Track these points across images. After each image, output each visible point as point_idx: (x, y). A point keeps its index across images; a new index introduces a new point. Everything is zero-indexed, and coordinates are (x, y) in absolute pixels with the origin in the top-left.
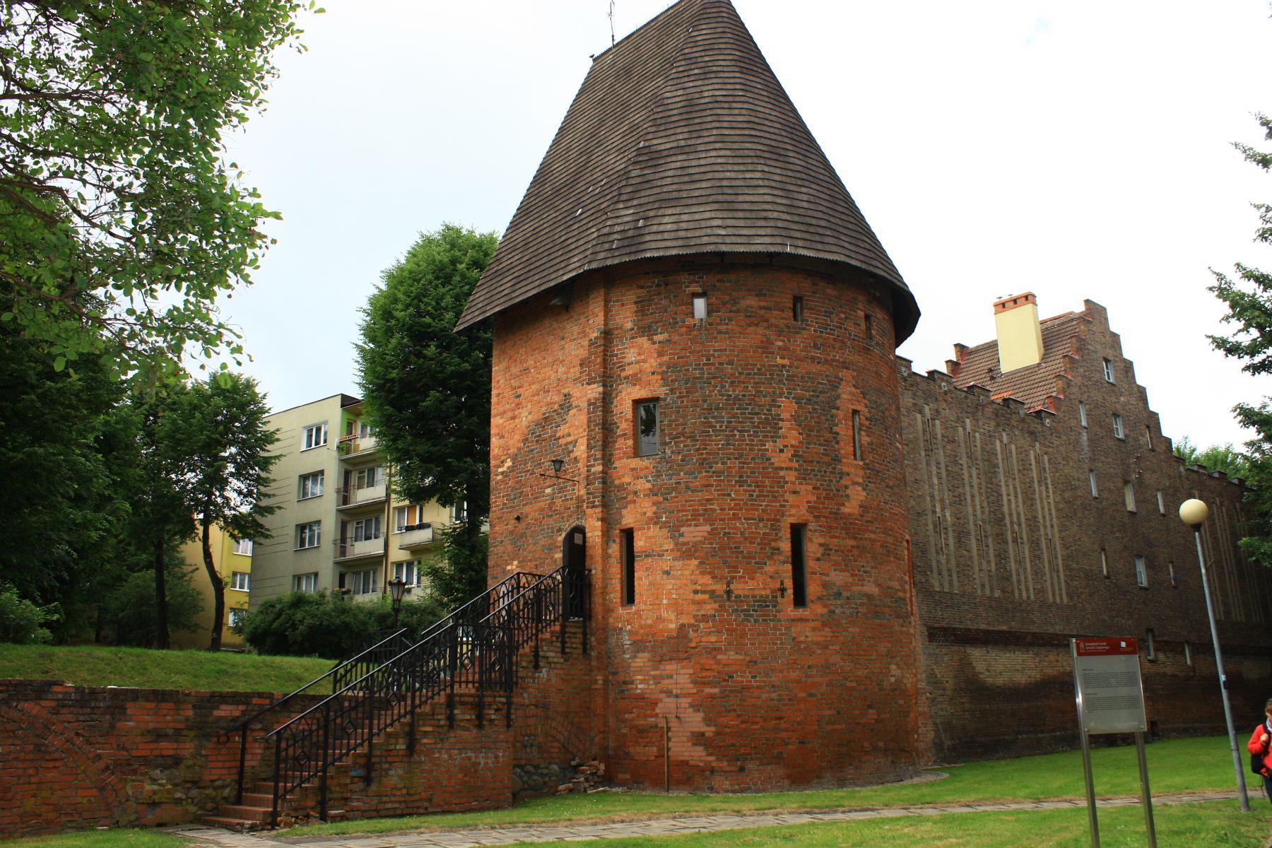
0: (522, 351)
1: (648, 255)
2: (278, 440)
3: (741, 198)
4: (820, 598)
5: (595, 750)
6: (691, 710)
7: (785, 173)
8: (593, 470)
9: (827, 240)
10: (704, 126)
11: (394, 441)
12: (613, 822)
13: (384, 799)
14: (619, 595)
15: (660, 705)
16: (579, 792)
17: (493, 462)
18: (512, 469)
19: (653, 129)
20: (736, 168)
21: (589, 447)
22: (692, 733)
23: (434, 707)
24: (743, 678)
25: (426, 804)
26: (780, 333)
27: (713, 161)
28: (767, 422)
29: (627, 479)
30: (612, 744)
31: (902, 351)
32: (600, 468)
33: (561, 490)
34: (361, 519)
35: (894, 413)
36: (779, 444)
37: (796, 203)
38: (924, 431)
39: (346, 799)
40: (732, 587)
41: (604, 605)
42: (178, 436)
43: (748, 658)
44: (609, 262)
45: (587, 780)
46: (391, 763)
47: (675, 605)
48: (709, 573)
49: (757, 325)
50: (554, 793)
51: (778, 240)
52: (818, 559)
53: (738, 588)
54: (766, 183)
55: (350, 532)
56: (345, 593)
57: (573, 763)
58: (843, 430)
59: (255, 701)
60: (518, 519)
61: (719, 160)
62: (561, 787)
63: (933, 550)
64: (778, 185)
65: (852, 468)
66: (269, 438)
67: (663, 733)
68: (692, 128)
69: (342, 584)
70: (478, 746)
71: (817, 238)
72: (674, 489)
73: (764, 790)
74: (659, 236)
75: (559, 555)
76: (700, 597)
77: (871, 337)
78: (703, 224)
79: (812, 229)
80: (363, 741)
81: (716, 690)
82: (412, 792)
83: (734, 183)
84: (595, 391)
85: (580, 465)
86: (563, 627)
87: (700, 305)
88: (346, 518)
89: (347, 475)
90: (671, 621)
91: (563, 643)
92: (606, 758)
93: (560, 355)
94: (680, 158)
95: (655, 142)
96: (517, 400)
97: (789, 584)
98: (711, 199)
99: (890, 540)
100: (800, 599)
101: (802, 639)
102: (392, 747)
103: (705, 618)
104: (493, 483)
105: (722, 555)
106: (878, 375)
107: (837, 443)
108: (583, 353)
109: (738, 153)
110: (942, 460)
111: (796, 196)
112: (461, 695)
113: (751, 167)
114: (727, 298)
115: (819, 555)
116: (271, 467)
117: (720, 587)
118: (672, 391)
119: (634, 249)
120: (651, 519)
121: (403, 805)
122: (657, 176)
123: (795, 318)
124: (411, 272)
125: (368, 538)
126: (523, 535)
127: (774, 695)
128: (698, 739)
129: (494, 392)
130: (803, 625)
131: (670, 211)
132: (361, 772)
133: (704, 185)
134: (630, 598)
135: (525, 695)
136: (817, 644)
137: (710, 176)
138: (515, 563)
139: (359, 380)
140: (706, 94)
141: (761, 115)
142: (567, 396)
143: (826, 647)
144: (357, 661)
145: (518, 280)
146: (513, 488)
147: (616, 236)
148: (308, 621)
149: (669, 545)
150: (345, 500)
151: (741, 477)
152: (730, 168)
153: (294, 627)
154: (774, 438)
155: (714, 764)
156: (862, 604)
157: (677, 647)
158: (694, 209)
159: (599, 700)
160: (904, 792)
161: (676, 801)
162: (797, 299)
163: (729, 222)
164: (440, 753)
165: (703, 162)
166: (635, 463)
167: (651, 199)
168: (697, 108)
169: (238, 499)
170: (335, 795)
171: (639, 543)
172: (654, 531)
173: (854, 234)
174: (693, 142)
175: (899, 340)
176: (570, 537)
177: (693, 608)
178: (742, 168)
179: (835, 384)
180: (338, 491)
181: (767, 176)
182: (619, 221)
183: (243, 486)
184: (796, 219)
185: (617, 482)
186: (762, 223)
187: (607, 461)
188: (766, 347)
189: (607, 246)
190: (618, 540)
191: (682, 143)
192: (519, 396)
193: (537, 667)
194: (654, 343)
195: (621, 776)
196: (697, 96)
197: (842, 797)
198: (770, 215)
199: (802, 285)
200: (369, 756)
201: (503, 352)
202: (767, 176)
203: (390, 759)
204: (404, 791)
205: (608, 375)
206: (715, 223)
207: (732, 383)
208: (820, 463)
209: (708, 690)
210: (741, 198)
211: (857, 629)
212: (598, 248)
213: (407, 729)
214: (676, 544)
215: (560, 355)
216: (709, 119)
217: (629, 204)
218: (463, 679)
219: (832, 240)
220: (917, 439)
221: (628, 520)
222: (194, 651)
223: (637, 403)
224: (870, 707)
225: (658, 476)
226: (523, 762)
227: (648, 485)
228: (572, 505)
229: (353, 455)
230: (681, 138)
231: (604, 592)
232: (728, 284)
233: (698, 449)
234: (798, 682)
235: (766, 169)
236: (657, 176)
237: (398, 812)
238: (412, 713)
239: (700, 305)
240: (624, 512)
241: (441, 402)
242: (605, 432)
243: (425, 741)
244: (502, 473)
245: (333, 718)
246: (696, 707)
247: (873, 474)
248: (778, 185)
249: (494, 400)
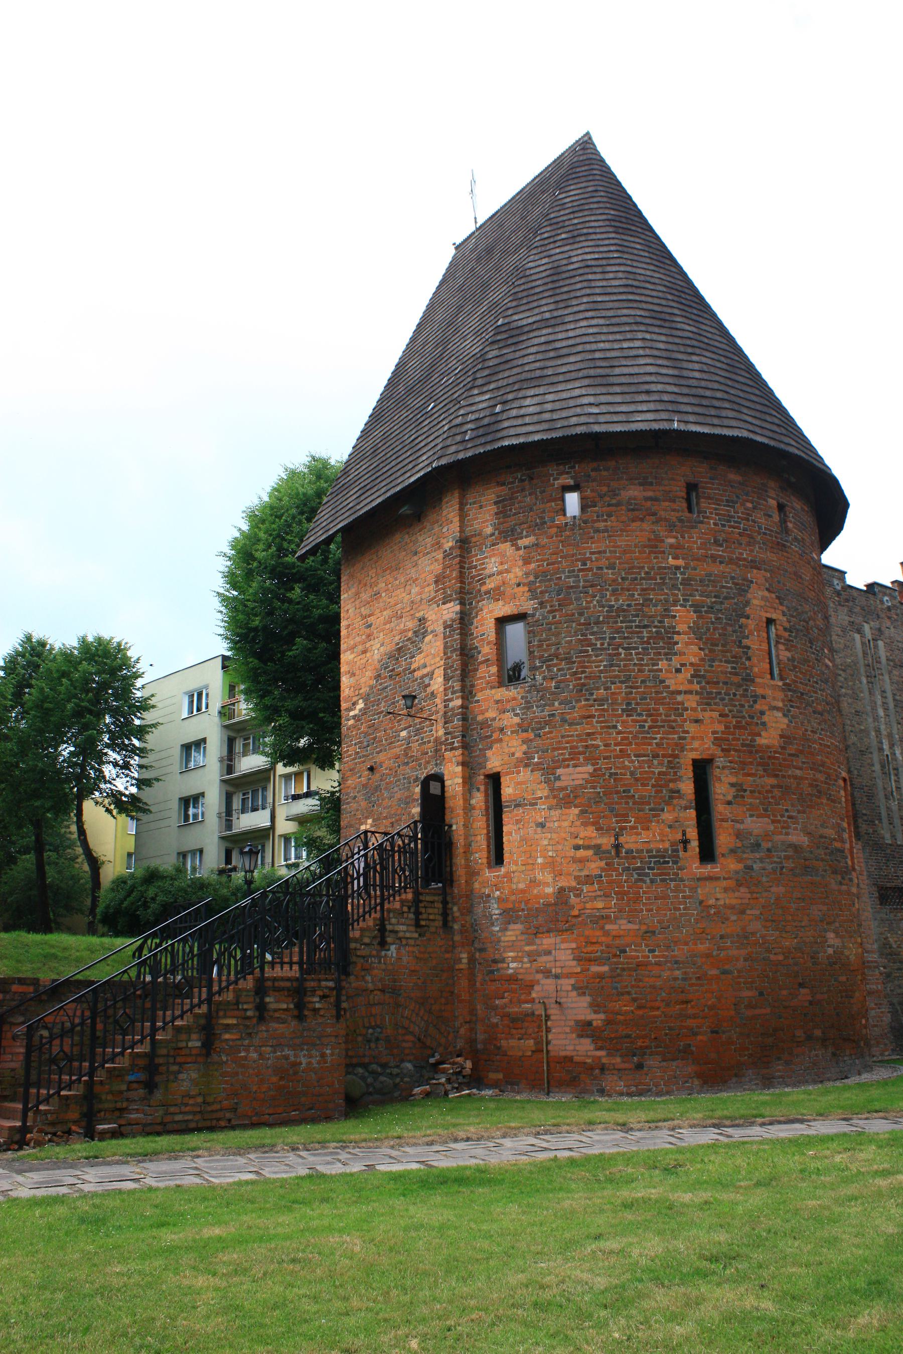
0: (372, 573)
1: (506, 443)
2: (153, 707)
3: (617, 371)
4: (733, 851)
5: (460, 1044)
6: (574, 993)
7: (671, 340)
8: (451, 705)
9: (724, 413)
10: (572, 295)
11: (262, 697)
12: (456, 1140)
13: (172, 1109)
14: (485, 854)
15: (536, 988)
16: (438, 1096)
17: (344, 705)
18: (364, 712)
19: (514, 304)
20: (611, 337)
21: (447, 678)
22: (577, 1022)
23: (238, 993)
24: (638, 952)
25: (228, 1115)
26: (671, 527)
27: (584, 331)
28: (658, 636)
29: (491, 714)
30: (481, 1037)
31: (830, 557)
32: (459, 702)
33: (418, 732)
34: (244, 789)
35: (821, 623)
36: (676, 662)
37: (685, 373)
38: (865, 654)
39: (121, 1110)
40: (622, 839)
41: (467, 866)
42: (46, 705)
43: (644, 928)
44: (461, 456)
45: (449, 1081)
46: (180, 1064)
47: (551, 864)
48: (593, 824)
49: (642, 520)
50: (406, 1098)
51: (664, 416)
52: (729, 803)
53: (629, 841)
54: (648, 352)
55: (236, 804)
56: (231, 870)
57: (432, 1060)
58: (755, 643)
59: (15, 988)
60: (371, 769)
61: (591, 331)
62: (417, 1090)
63: (881, 795)
64: (664, 354)
65: (770, 690)
66: (144, 706)
67: (541, 1022)
68: (558, 298)
69: (228, 860)
70: (298, 1041)
71: (713, 412)
72: (546, 723)
73: (668, 1093)
74: (520, 421)
75: (416, 810)
76: (581, 853)
77: (787, 531)
78: (572, 403)
79: (705, 402)
80: (144, 1038)
81: (605, 968)
82: (210, 1099)
83: (609, 354)
84: (451, 610)
85: (438, 701)
86: (417, 894)
87: (572, 501)
88: (231, 789)
89: (231, 742)
90: (547, 884)
91: (417, 913)
92: (474, 1054)
93: (413, 573)
94: (544, 332)
95: (516, 317)
96: (368, 631)
97: (693, 834)
98: (581, 374)
99: (821, 777)
100: (707, 854)
101: (712, 902)
102: (183, 1044)
104: (344, 730)
105: (608, 801)
106: (798, 576)
107: (749, 659)
108: (437, 568)
109: (614, 321)
110: (888, 687)
111: (685, 365)
112: (275, 979)
113: (629, 336)
114: (605, 489)
115: (729, 798)
116: (147, 737)
117: (606, 841)
118: (541, 604)
119: (489, 438)
120: (520, 760)
121: (198, 1117)
122: (518, 354)
123: (690, 509)
124: (272, 508)
125: (255, 809)
126: (377, 788)
127: (678, 973)
128: (584, 1029)
129: (344, 623)
130: (712, 886)
131: (532, 392)
132: (142, 1076)
133: (572, 359)
134: (498, 857)
135: (369, 978)
136: (732, 907)
137: (580, 348)
138: (370, 821)
139: (221, 631)
140: (574, 259)
141: (642, 278)
142: (423, 620)
143: (743, 912)
144: (146, 939)
145: (365, 490)
146: (366, 734)
147: (470, 426)
148: (161, 898)
149: (542, 791)
150: (230, 769)
151: (629, 704)
152: (603, 338)
153: (145, 905)
154: (669, 655)
155: (604, 1061)
156: (787, 858)
157: (556, 916)
158: (560, 387)
159: (464, 983)
160: (847, 1095)
161: (559, 1106)
162: (691, 488)
163: (603, 399)
164: (247, 1051)
165: (571, 334)
166: (502, 693)
167: (511, 380)
168: (564, 276)
169: (114, 772)
170: (106, 1106)
171: (508, 791)
172: (525, 774)
173: (758, 407)
174: (560, 313)
175: (825, 540)
176: (425, 783)
177: (574, 868)
178: (618, 337)
179: (742, 588)
180: (221, 760)
181: (649, 344)
182: (474, 408)
183: (118, 758)
184: (685, 390)
185: (480, 718)
186: (644, 397)
187: (467, 693)
188: (654, 545)
189: (458, 438)
190: (482, 788)
191: (547, 315)
192: (370, 626)
193: (383, 944)
194: (518, 549)
195: (493, 1076)
196: (565, 262)
197: (764, 1103)
198: (653, 387)
199: (699, 471)
200: (151, 1056)
201: (352, 576)
202: (649, 344)
203: (179, 1059)
204: (200, 1100)
205: (465, 591)
206: (585, 400)
207: (614, 591)
208: (725, 683)
209: (595, 969)
210: (617, 371)
211: (781, 890)
212: (449, 442)
213: (202, 1021)
214: (552, 790)
215: (413, 573)
216: (579, 286)
217: (485, 389)
218: (286, 960)
219: (731, 414)
220: (855, 663)
221: (494, 762)
222: (23, 934)
224: (801, 985)
225: (528, 708)
226: (367, 1060)
227: (517, 720)
228: (430, 748)
229: (236, 720)
230: (546, 310)
231: (468, 850)
232: (605, 473)
233: (575, 673)
234: (709, 956)
235: (648, 336)
236: (518, 354)
237: (192, 1125)
238: (209, 1000)
239: (572, 501)
240: (489, 753)
241: (309, 650)
242: (464, 659)
243: (227, 1036)
244: (354, 717)
245: (109, 1005)
246: (580, 990)
247: (795, 697)
248: (664, 354)
249: (343, 632)
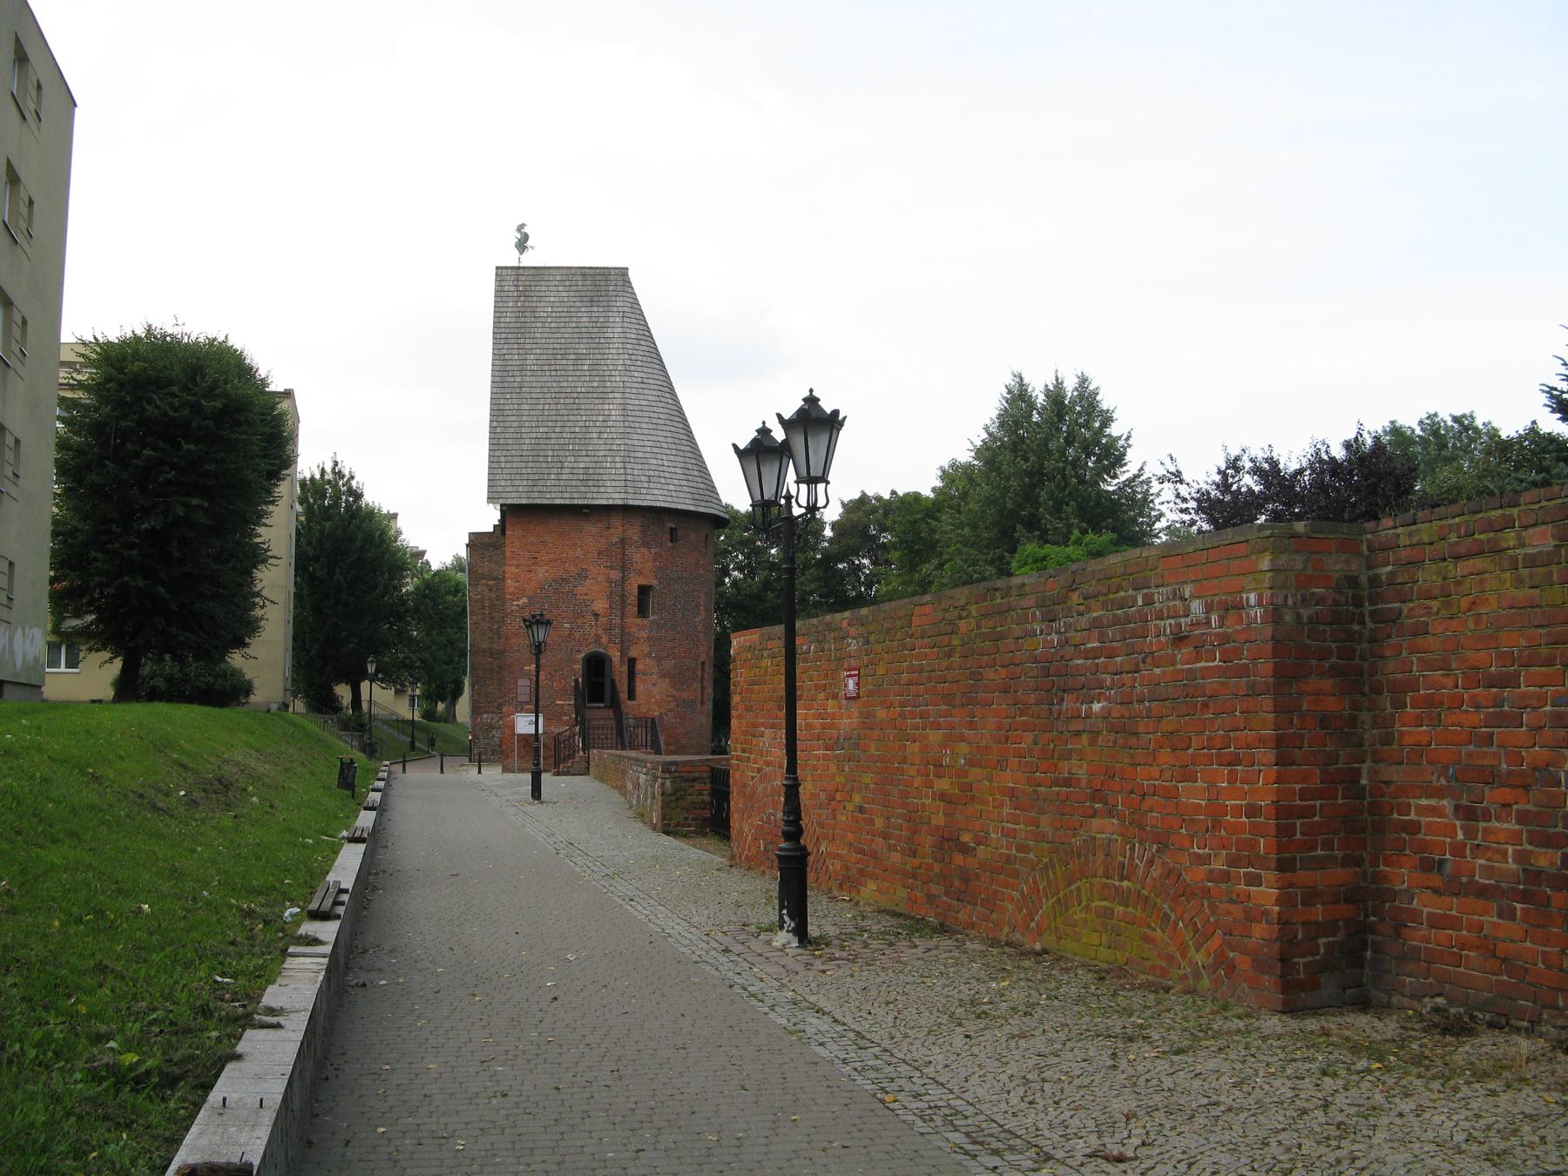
75: (578, 667)
134: (632, 695)
166: (639, 621)
171: (639, 666)
221: (633, 653)
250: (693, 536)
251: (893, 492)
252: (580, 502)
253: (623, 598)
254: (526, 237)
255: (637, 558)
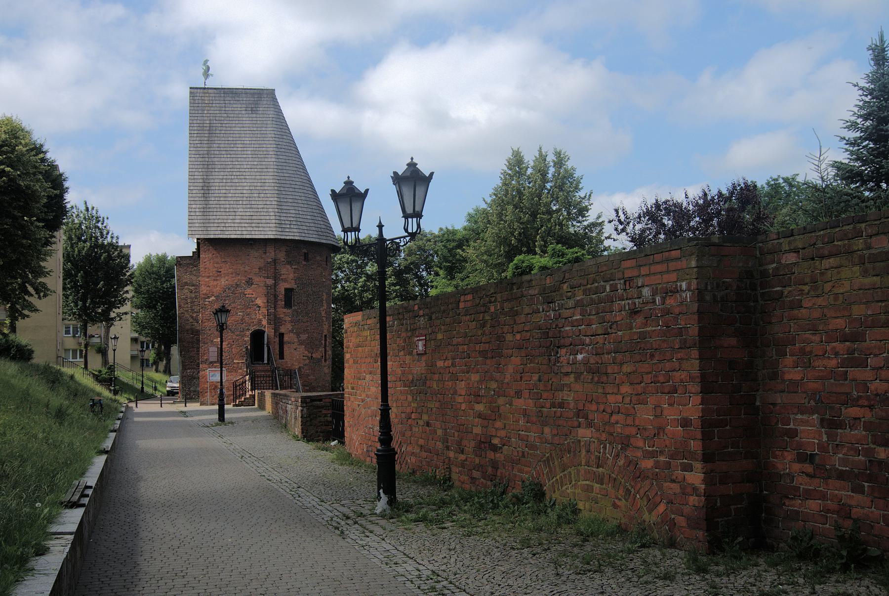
75: (247, 339)
103: (306, 365)
166: (285, 310)
171: (286, 338)
172: (291, 335)
221: (282, 330)
223: (286, 290)
250: (318, 258)
251: (441, 229)
252: (248, 237)
253: (275, 296)
254: (208, 68)
255: (283, 271)
